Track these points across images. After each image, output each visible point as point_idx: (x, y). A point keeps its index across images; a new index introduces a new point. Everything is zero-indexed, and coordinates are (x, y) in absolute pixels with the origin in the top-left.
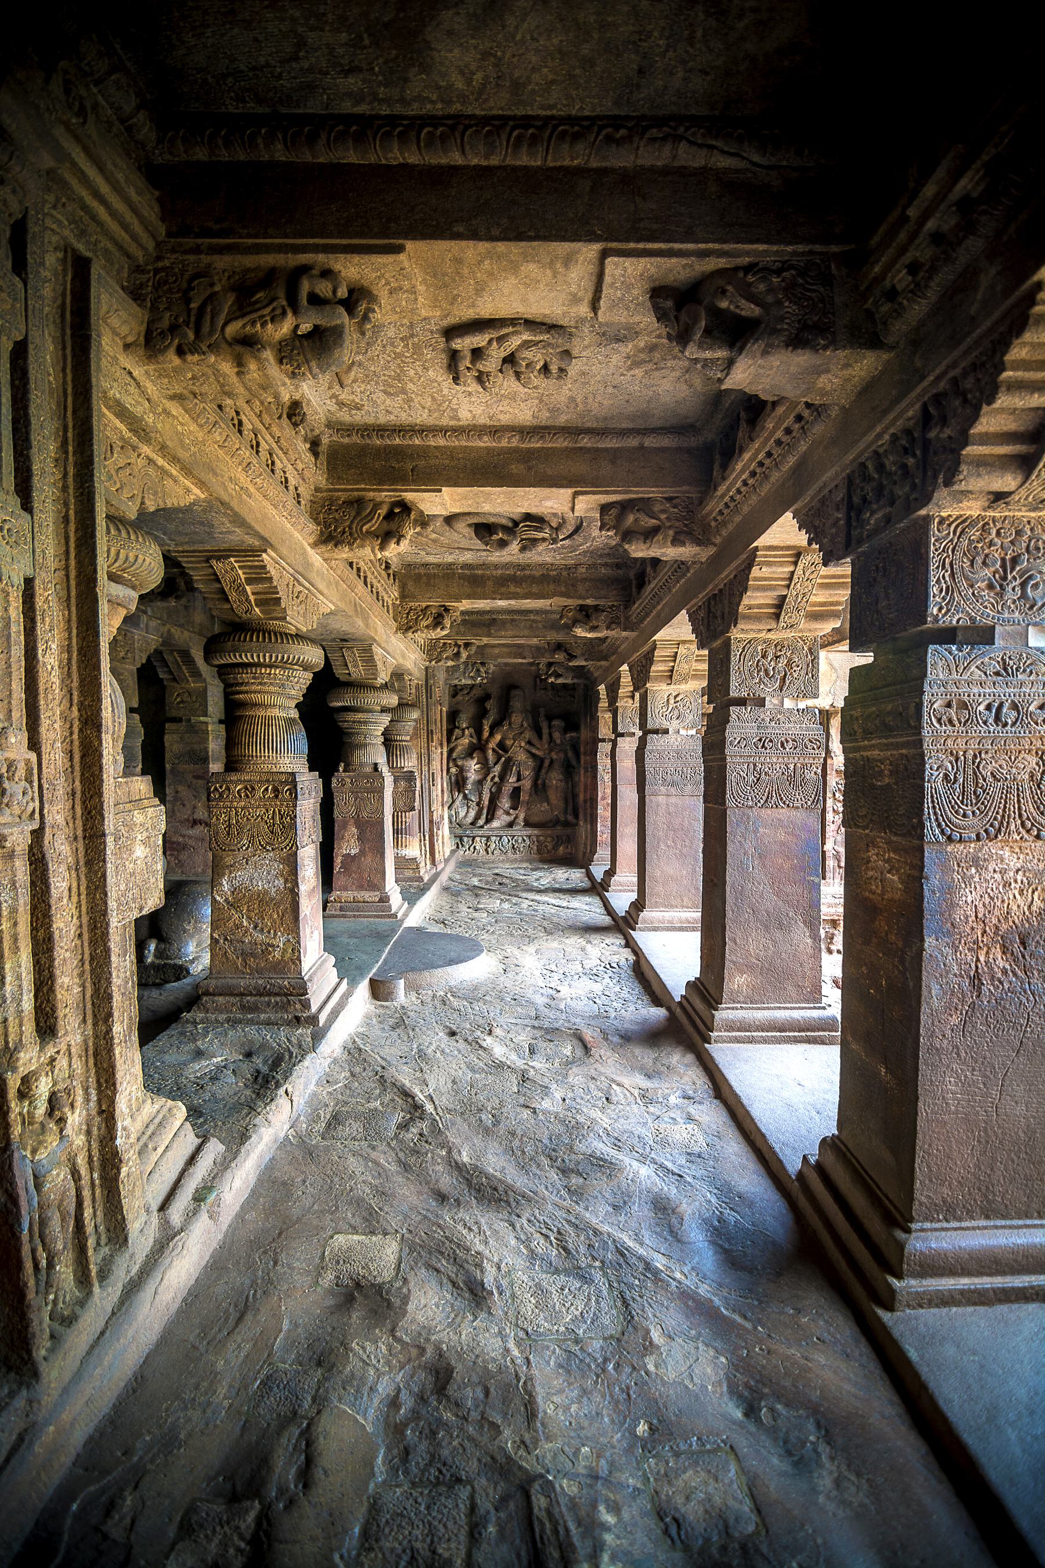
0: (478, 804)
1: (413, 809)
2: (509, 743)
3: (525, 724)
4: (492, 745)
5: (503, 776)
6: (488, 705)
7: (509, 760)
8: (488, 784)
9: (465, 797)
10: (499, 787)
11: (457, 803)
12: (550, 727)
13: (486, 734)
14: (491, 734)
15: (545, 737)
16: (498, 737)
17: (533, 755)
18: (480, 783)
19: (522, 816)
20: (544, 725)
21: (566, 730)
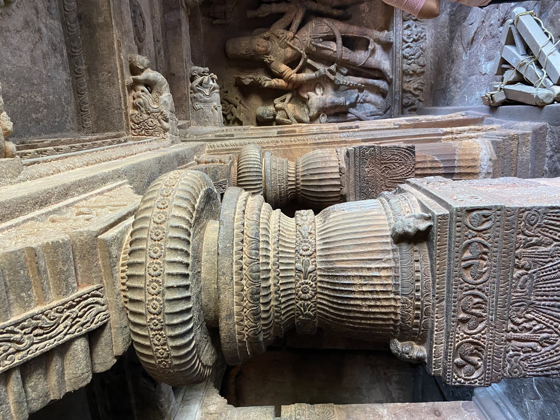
0: (361, 90)
1: (411, 150)
2: (289, 53)
3: (266, 35)
4: (291, 73)
7: (310, 55)
10: (343, 63)
13: (281, 82)
14: (280, 76)
17: (303, 24)
18: (337, 88)
19: (377, 34)
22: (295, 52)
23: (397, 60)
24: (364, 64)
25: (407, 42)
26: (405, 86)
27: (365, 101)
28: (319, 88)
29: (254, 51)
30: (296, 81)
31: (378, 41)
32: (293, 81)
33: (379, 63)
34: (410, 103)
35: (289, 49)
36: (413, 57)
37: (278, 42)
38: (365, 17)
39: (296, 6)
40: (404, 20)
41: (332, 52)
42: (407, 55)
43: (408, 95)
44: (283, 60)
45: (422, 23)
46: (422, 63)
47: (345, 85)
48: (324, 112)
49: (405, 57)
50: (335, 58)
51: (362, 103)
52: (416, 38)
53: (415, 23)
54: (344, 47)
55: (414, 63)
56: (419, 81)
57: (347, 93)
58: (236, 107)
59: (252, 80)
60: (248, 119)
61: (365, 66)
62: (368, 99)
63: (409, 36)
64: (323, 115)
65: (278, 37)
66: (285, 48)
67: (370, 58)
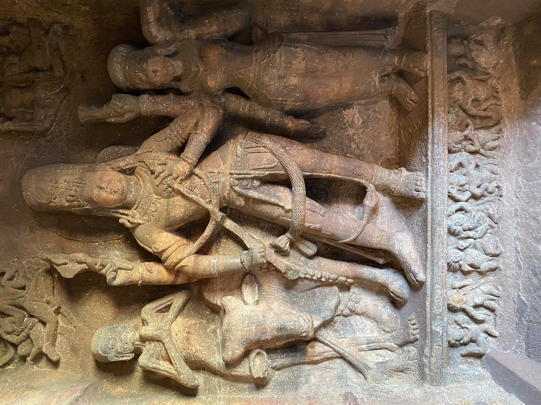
0: (344, 287)
2: (179, 209)
5: (276, 227)
6: (70, 269)
8: (294, 264)
9: (326, 324)
10: (307, 235)
11: (343, 344)
12: (136, 92)
15: (164, 105)
16: (165, 241)
18: (290, 284)
20: (123, 108)
21: (140, 43)
22: (194, 207)
23: (437, 241)
24: (355, 239)
25: (456, 201)
26: (456, 298)
27: (353, 312)
28: (251, 283)
29: (90, 201)
30: (194, 275)
31: (386, 190)
32: (186, 273)
33: (389, 239)
34: (466, 339)
35: (178, 200)
36: (471, 233)
37: (152, 183)
38: (355, 137)
39: (201, 105)
40: (450, 152)
41: (281, 211)
42: (459, 229)
43: (461, 317)
44: (163, 222)
45: (490, 160)
46: (491, 250)
47: (311, 280)
48: (261, 347)
49: (452, 233)
50: (289, 223)
51: (346, 316)
52: (478, 192)
53: (474, 160)
54: (309, 201)
55: (475, 247)
56: (486, 288)
57: (314, 295)
58: (44, 324)
59: (85, 266)
60: (74, 350)
61: (359, 242)
62: (359, 307)
63: (462, 188)
64: (258, 354)
65: (153, 173)
66: (169, 197)
67: (370, 226)
